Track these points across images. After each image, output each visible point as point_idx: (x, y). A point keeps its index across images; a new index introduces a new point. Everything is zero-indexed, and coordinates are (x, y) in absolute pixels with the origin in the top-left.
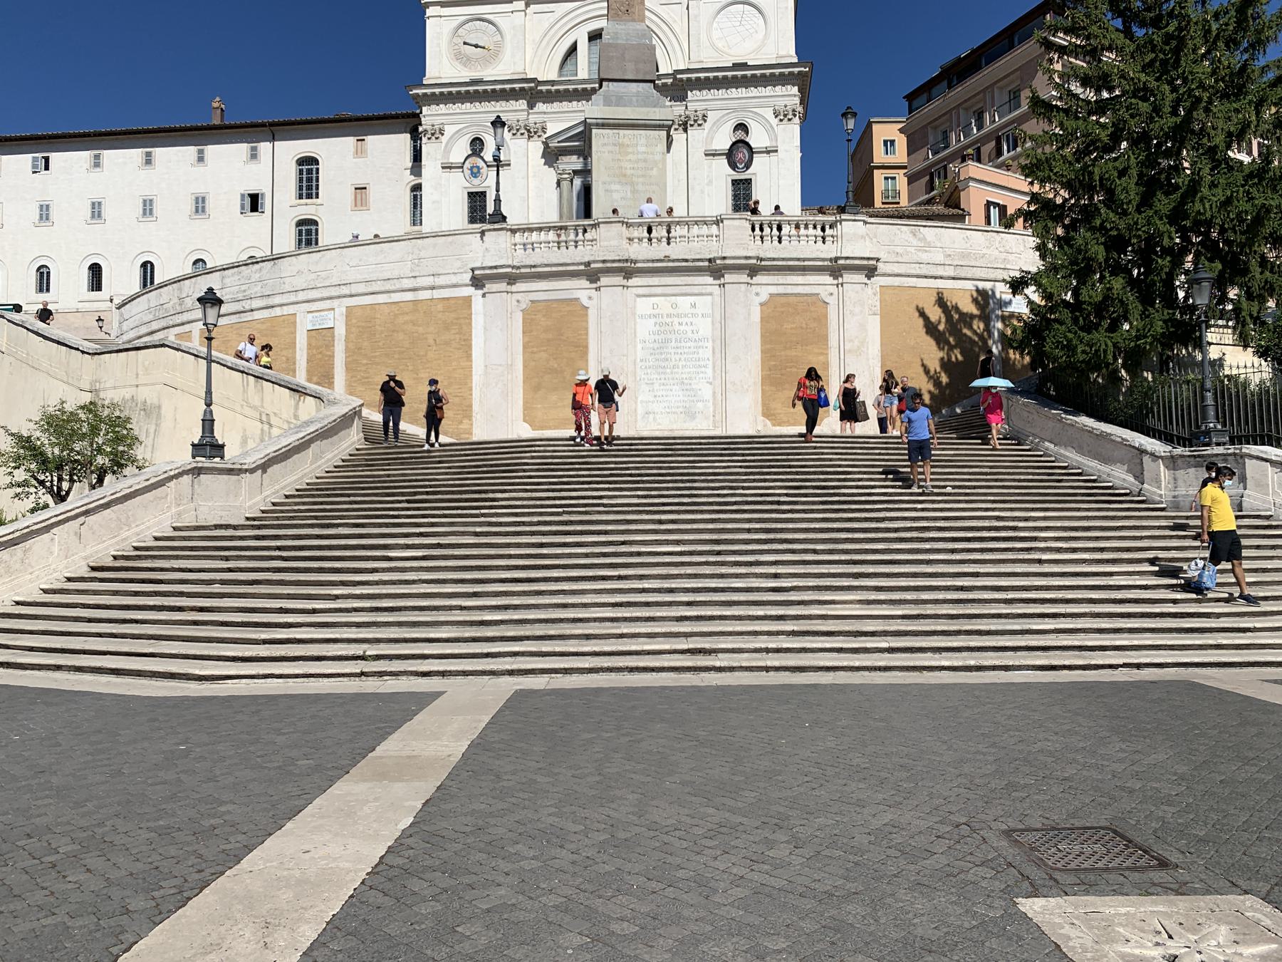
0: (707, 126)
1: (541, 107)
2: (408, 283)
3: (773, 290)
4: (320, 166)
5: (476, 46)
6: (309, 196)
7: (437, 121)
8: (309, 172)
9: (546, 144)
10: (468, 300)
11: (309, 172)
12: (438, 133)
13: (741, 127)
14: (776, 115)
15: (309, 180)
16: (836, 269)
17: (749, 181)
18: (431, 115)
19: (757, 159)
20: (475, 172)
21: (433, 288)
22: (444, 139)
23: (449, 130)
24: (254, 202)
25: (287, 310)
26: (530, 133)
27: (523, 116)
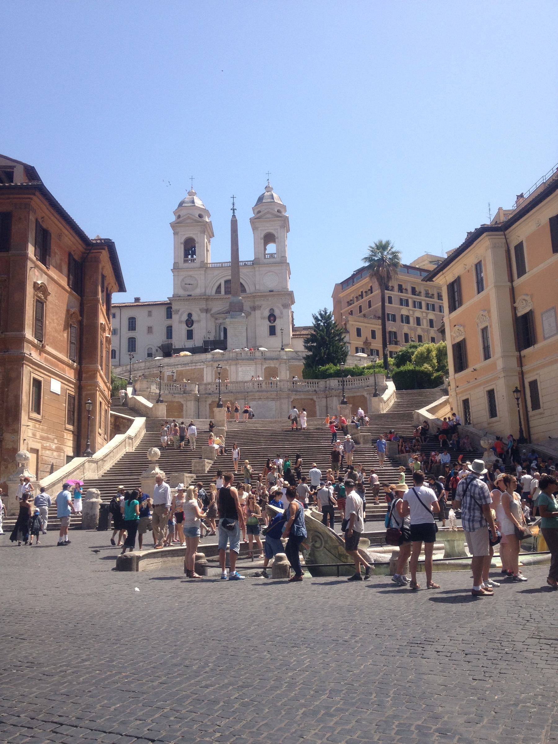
0: (262, 309)
1: (210, 303)
3: (267, 366)
5: (189, 284)
6: (132, 330)
8: (132, 322)
10: (203, 369)
11: (132, 322)
12: (177, 311)
13: (272, 310)
14: (283, 306)
15: (132, 324)
17: (275, 326)
18: (174, 307)
19: (277, 321)
21: (195, 366)
22: (180, 313)
26: (207, 311)
27: (204, 306)
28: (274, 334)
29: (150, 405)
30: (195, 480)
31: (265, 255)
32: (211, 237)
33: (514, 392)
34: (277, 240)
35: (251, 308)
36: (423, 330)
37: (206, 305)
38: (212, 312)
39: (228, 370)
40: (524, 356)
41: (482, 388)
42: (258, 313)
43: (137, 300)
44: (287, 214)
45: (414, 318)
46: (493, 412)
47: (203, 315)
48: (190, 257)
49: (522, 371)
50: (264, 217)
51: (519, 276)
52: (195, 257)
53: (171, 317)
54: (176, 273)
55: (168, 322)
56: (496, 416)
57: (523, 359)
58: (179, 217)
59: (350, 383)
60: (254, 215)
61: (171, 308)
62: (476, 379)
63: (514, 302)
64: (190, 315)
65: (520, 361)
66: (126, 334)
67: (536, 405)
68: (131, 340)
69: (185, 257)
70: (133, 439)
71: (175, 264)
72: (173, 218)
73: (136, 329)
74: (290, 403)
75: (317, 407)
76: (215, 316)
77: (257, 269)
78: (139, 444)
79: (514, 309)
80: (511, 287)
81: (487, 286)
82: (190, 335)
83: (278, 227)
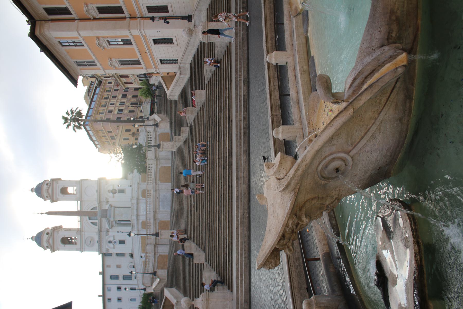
1: (103, 229)
2: (139, 244)
3: (141, 197)
4: (112, 274)
5: (91, 242)
6: (118, 277)
7: (105, 250)
9: (110, 229)
14: (106, 184)
16: (138, 188)
18: (104, 251)
20: (115, 242)
22: (108, 248)
23: (107, 247)
24: (119, 288)
25: (142, 262)
26: (108, 231)
27: (105, 233)
28: (124, 190)
29: (158, 280)
30: (209, 263)
31: (74, 194)
32: (62, 227)
33: (153, 21)
34: (65, 187)
35: (107, 204)
36: (127, 101)
37: (104, 232)
38: (109, 228)
39: (143, 221)
40: (130, 15)
41: (153, 49)
42: (110, 200)
43: (100, 273)
44: (50, 180)
45: (120, 107)
46: (169, 41)
47: (110, 234)
48: (73, 241)
49: (141, 17)
50: (50, 194)
51: (70, 13)
52: (73, 238)
53: (111, 253)
54: (83, 250)
55: (114, 256)
56: (172, 39)
57: (131, 17)
58: (47, 247)
59: (150, 143)
60: (49, 200)
61: (105, 253)
62: (146, 53)
63: (90, 19)
64: (110, 242)
65: (133, 18)
66: (121, 282)
67: (164, 9)
68: (124, 278)
69: (73, 244)
70: (178, 300)
71: (77, 250)
72: (49, 251)
73: (118, 275)
74: (162, 183)
75: (165, 165)
76: (112, 227)
77: (83, 200)
78: (182, 295)
79: (95, 19)
80: (79, 21)
81: (77, 38)
82: (122, 242)
83: (58, 185)
